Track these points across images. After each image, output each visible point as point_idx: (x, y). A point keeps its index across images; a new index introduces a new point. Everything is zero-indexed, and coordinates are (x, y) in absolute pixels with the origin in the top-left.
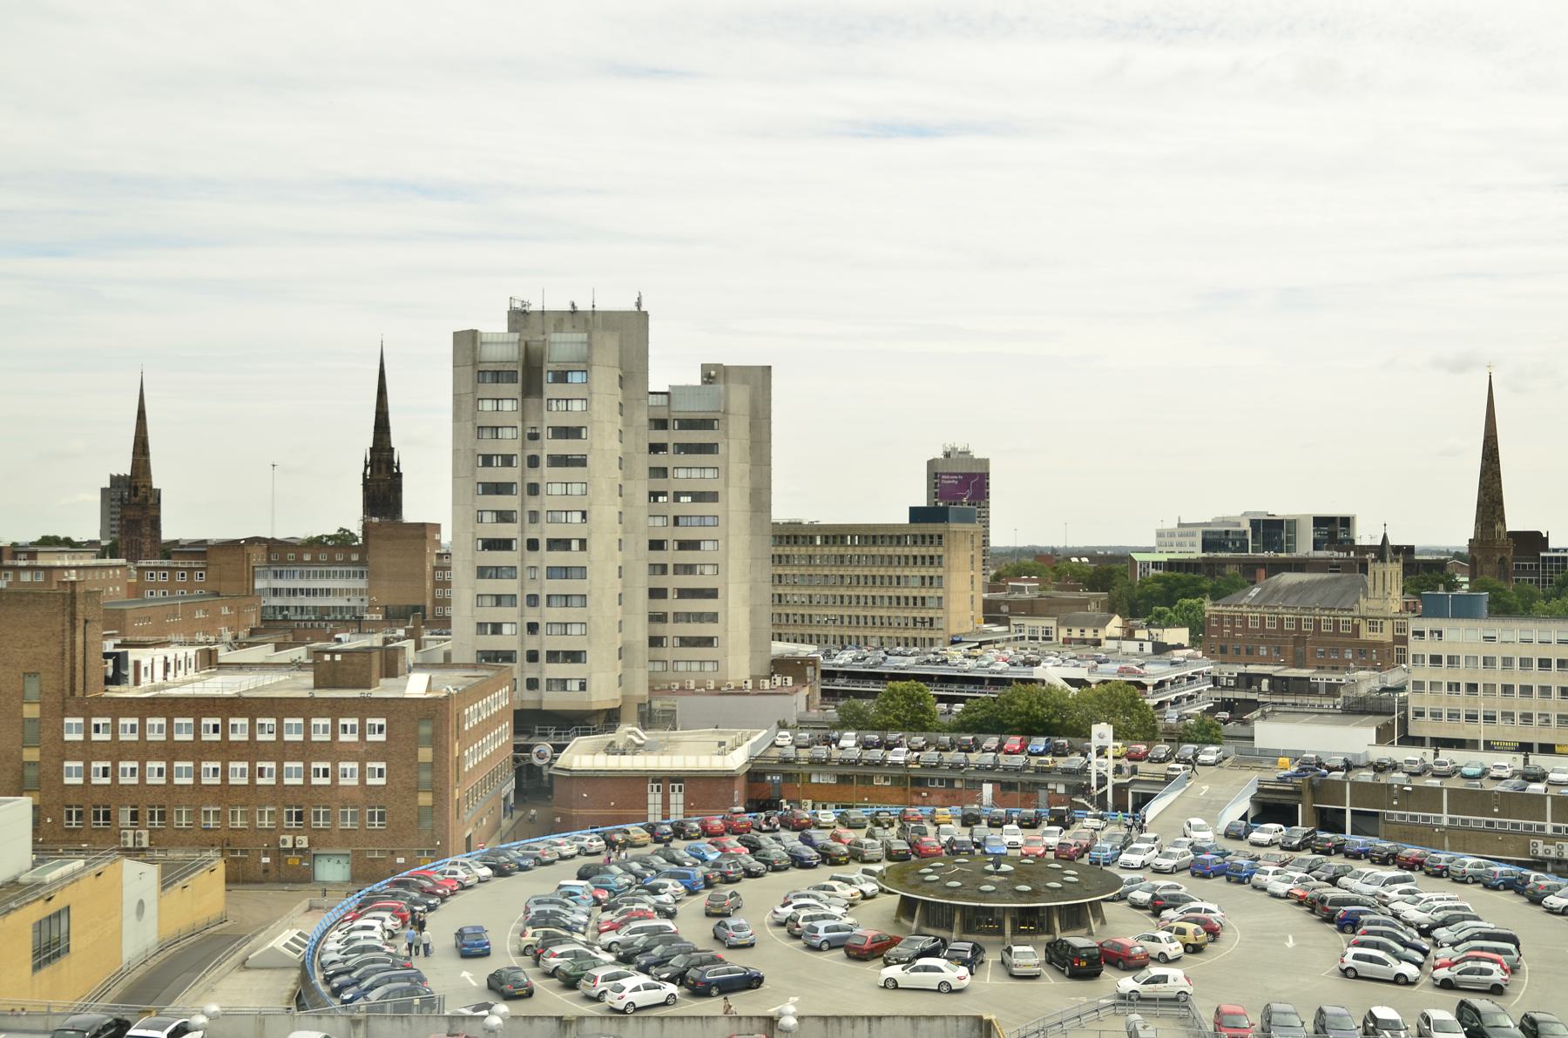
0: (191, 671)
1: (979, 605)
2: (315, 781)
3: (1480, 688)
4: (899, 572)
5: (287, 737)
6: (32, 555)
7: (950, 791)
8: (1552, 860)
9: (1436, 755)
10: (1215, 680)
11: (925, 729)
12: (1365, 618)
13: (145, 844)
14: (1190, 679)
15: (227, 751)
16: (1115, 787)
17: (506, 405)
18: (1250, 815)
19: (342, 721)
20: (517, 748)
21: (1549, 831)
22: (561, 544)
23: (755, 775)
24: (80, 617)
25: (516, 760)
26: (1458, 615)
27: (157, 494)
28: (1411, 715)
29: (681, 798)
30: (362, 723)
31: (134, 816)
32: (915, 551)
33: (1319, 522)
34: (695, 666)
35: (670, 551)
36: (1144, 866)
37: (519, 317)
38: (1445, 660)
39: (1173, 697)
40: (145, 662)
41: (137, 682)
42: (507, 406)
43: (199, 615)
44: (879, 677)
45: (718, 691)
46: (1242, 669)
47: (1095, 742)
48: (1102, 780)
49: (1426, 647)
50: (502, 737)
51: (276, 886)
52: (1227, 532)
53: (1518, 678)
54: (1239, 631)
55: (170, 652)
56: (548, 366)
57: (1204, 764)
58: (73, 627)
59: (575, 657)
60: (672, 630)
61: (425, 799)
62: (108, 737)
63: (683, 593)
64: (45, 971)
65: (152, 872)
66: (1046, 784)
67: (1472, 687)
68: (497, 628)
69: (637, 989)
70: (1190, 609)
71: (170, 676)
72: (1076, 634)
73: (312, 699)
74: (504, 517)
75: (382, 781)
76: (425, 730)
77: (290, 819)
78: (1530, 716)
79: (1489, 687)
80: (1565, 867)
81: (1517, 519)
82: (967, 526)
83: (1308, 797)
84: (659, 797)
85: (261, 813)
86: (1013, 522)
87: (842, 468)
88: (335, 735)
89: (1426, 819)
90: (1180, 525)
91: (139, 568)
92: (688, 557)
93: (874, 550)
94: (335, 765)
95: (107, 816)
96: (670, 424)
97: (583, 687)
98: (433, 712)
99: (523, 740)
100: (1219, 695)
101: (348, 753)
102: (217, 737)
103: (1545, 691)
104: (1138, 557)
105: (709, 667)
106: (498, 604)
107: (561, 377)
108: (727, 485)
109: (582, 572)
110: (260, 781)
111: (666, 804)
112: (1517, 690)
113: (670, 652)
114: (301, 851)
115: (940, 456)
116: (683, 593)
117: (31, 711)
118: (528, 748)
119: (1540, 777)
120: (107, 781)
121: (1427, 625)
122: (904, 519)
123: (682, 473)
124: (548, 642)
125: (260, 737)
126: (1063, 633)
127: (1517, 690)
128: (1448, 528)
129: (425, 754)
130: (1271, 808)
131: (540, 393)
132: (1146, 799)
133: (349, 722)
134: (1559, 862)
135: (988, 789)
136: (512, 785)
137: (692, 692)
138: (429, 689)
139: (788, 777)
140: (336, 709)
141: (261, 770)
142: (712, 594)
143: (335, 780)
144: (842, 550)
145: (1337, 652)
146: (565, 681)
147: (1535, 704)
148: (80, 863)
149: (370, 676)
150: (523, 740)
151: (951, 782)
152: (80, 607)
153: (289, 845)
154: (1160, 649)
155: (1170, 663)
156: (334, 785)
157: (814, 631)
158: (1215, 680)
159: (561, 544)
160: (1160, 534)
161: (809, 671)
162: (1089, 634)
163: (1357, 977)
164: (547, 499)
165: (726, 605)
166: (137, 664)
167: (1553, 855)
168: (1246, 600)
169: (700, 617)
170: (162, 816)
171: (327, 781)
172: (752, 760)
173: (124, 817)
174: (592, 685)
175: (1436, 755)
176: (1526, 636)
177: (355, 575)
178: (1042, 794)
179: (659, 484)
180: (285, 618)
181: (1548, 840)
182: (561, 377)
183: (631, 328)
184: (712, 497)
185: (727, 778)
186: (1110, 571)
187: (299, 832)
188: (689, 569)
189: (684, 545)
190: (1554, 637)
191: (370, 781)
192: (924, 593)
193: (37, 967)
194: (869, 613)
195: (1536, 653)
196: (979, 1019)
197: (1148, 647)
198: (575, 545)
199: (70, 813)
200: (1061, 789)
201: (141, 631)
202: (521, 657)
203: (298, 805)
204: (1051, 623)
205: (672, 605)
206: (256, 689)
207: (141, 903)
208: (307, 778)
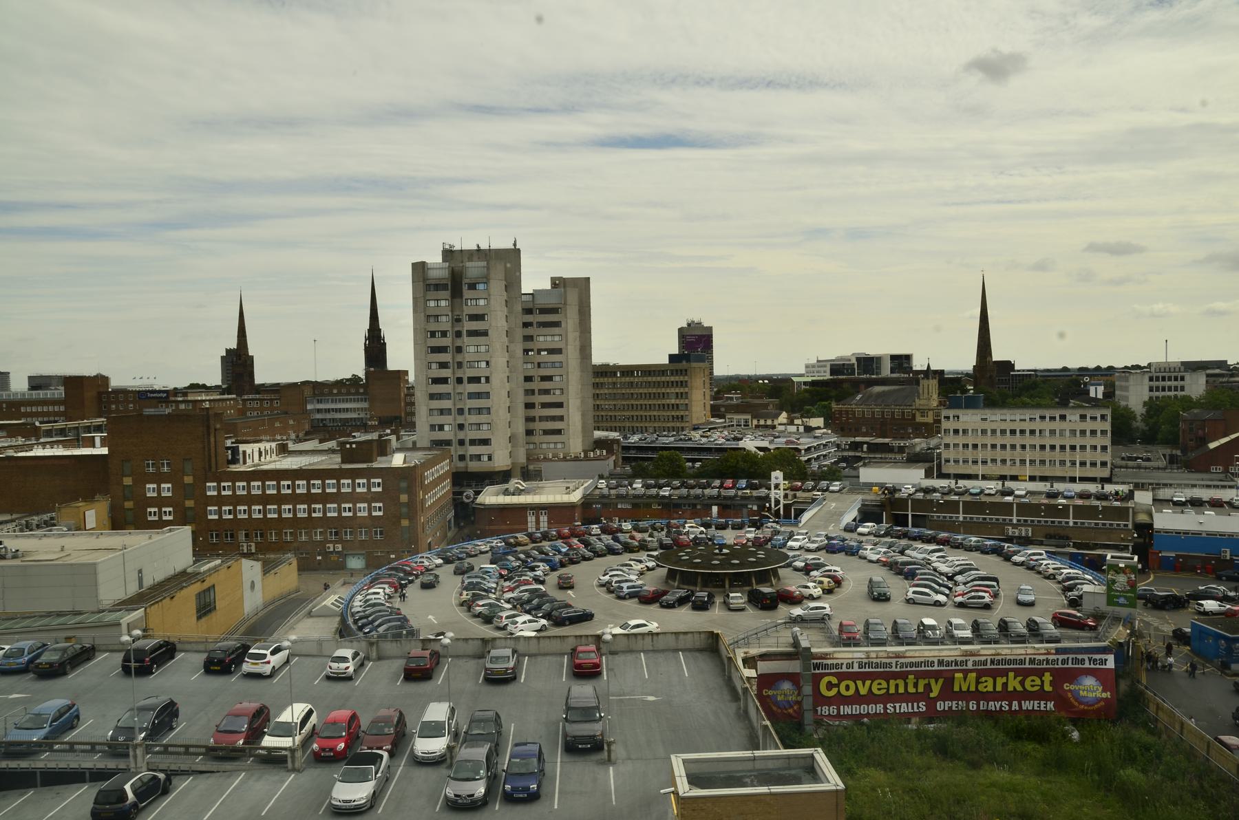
0: (274, 456)
1: (708, 408)
2: (344, 514)
6: (185, 394)
10: (838, 446)
15: (295, 499)
20: (454, 493)
22: (476, 380)
23: (587, 502)
25: (454, 500)
29: (546, 518)
31: (247, 536)
32: (673, 379)
33: (893, 358)
34: (552, 446)
36: (800, 548)
37: (448, 254)
40: (249, 451)
41: (245, 462)
45: (565, 459)
47: (773, 482)
48: (777, 502)
50: (446, 486)
53: (999, 441)
55: (262, 446)
56: (465, 281)
57: (833, 492)
58: (209, 434)
59: (486, 442)
62: (230, 493)
63: (545, 405)
64: (204, 619)
65: (258, 566)
67: (975, 446)
68: (441, 428)
70: (825, 407)
72: (762, 422)
74: (443, 365)
75: (381, 514)
76: (404, 485)
81: (998, 355)
82: (701, 364)
86: (728, 361)
87: (629, 336)
88: (354, 489)
92: (546, 385)
93: (650, 379)
94: (355, 505)
97: (490, 458)
99: (457, 489)
102: (290, 491)
103: (1013, 447)
105: (559, 446)
107: (472, 286)
109: (487, 395)
111: (538, 522)
113: (537, 438)
116: (545, 405)
117: (188, 480)
118: (461, 493)
119: (1011, 493)
120: (231, 517)
121: (951, 413)
122: (666, 361)
123: (541, 339)
125: (313, 491)
126: (755, 422)
128: (962, 360)
130: (866, 514)
131: (461, 297)
132: (803, 511)
133: (361, 481)
134: (1020, 537)
135: (715, 509)
136: (451, 515)
142: (560, 405)
143: (355, 513)
146: (479, 456)
147: (1008, 454)
148: (218, 562)
150: (457, 489)
151: (694, 505)
152: (212, 422)
154: (809, 429)
155: (813, 436)
157: (618, 425)
158: (838, 446)
159: (476, 380)
160: (807, 366)
161: (615, 447)
162: (769, 422)
163: (914, 603)
166: (244, 452)
169: (554, 418)
172: (584, 497)
173: (242, 537)
178: (745, 511)
180: (325, 425)
181: (1015, 526)
182: (472, 286)
183: (512, 257)
184: (558, 351)
185: (570, 507)
187: (337, 542)
188: (547, 392)
190: (1018, 417)
191: (374, 514)
193: (199, 618)
195: (1008, 426)
196: (712, 633)
197: (802, 429)
198: (483, 380)
200: (755, 508)
201: (244, 435)
202: (455, 443)
204: (749, 417)
205: (539, 412)
208: (340, 513)
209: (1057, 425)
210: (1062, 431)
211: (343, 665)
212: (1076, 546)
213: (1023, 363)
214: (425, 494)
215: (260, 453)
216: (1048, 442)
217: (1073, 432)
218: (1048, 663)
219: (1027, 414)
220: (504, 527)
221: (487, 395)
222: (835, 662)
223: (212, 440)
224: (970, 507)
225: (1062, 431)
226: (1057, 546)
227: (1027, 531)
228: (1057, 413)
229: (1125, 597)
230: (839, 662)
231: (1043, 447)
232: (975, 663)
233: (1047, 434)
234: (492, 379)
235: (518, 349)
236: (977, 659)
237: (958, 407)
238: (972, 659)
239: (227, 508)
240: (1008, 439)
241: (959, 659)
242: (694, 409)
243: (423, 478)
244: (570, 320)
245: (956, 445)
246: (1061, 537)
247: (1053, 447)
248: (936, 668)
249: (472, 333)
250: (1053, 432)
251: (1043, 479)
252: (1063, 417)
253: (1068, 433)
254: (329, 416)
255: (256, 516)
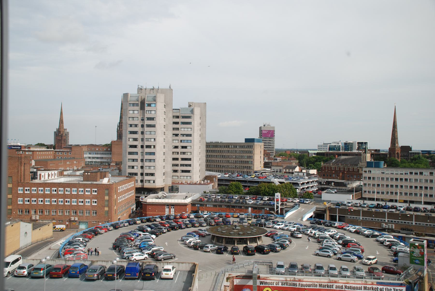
0: (56, 177)
1: (263, 163)
2: (79, 204)
3: (380, 185)
4: (242, 155)
5: (73, 193)
6: (29, 148)
7: (241, 209)
8: (387, 229)
9: (364, 202)
10: (320, 183)
11: (239, 194)
12: (361, 167)
13: (38, 219)
14: (311, 182)
15: (58, 196)
16: (281, 209)
17: (134, 113)
18: (313, 216)
19: (86, 189)
20: (136, 197)
21: (386, 221)
23: (193, 204)
24: (23, 163)
25: (136, 200)
26: (375, 167)
27: (68, 133)
28: (363, 192)
29: (173, 210)
30: (91, 190)
31: (35, 212)
32: (213, 149)
33: (358, 143)
34: (185, 177)
35: (179, 149)
36: (280, 229)
37: (140, 89)
38: (372, 178)
39: (306, 187)
41: (40, 179)
42: (136, 112)
43: (68, 163)
44: (234, 181)
45: (190, 184)
46: (327, 180)
47: (276, 197)
48: (277, 207)
49: (367, 175)
50: (132, 193)
51: (70, 230)
52: (335, 146)
53: (390, 183)
54: (329, 170)
55: (53, 172)
56: (146, 102)
57: (305, 203)
58: (21, 165)
59: (152, 175)
60: (180, 168)
61: (106, 209)
62: (29, 192)
63: (183, 159)
65: (30, 226)
66: (264, 208)
67: (378, 185)
68: (133, 167)
69: (137, 256)
70: (319, 165)
71: (50, 178)
72: (287, 171)
73: (79, 183)
74: (135, 140)
75: (96, 204)
76: (106, 192)
77: (87, 213)
78: (393, 192)
79: (383, 185)
80: (390, 230)
83: (328, 212)
84: (168, 209)
85: (66, 212)
86: (281, 143)
88: (84, 193)
89: (356, 218)
90: (324, 144)
91: (56, 152)
92: (184, 150)
93: (242, 149)
94: (84, 200)
95: (29, 212)
96: (180, 117)
97: (154, 182)
98: (108, 188)
99: (138, 195)
100: (320, 186)
101: (88, 197)
102: (56, 193)
103: (397, 186)
104: (310, 152)
105: (189, 178)
106: (133, 161)
108: (194, 132)
109: (154, 154)
110: (66, 204)
111: (170, 211)
112: (390, 186)
114: (76, 221)
115: (262, 126)
116: (183, 159)
118: (139, 197)
119: (396, 208)
120: (42, 203)
121: (367, 169)
123: (183, 129)
124: (146, 171)
125: (66, 193)
126: (284, 170)
127: (390, 186)
128: (384, 146)
129: (107, 198)
130: (319, 215)
132: (287, 212)
133: (61, 189)
134: (389, 229)
135: (250, 209)
136: (134, 207)
137: (184, 184)
138: (109, 181)
139: (201, 205)
140: (85, 186)
141: (66, 201)
142: (190, 159)
143: (85, 204)
144: (228, 149)
145: (352, 176)
147: (394, 190)
148: (9, 223)
149: (97, 179)
150: (138, 195)
151: (241, 207)
152: (23, 160)
153: (73, 220)
154: (308, 174)
155: (308, 178)
156: (84, 205)
157: (210, 169)
158: (320, 183)
160: (319, 146)
161: (214, 179)
162: (291, 171)
163: (319, 256)
164: (145, 135)
165: (193, 162)
166: (40, 175)
167: (387, 227)
168: (331, 163)
169: (186, 165)
170: (42, 212)
171: (82, 204)
172: (193, 201)
173: (32, 212)
174: (156, 182)
175: (364, 202)
176: (397, 173)
177: (109, 154)
178: (263, 210)
179: (176, 132)
180: (91, 164)
181: (386, 223)
182: (149, 105)
184: (190, 135)
185: (185, 205)
186: (304, 155)
187: (75, 216)
188: (184, 153)
189: (183, 147)
190: (399, 173)
191: (93, 204)
192: (248, 160)
194: (219, 164)
195: (394, 177)
196: (194, 264)
197: (305, 174)
198: (152, 147)
199: (19, 211)
200: (268, 209)
202: (139, 174)
203: (76, 210)
204: (282, 168)
205: (180, 162)
206: (69, 181)
207: (26, 233)
208: (78, 203)
209: (418, 177)
210: (421, 180)
211: (22, 271)
212: (416, 234)
213: (416, 148)
214: (118, 196)
215: (49, 175)
216: (414, 185)
217: (426, 181)
218: (328, 287)
219: (404, 171)
220: (154, 213)
221: (154, 154)
222: (270, 281)
223: (23, 168)
224: (365, 213)
225: (421, 180)
226: (406, 234)
227: (392, 226)
228: (418, 171)
229: (419, 260)
230: (272, 281)
231: (411, 187)
232: (337, 287)
233: (413, 181)
234: (156, 147)
235: (170, 133)
236: (338, 284)
237: (372, 167)
238: (335, 284)
239: (27, 199)
240: (394, 183)
241: (329, 284)
242: (255, 164)
243: (117, 190)
244: (196, 120)
245: (369, 184)
246: (408, 230)
247: (416, 187)
248: (318, 288)
249: (149, 126)
250: (416, 180)
251: (382, 200)
252: (421, 173)
253: (424, 181)
254: (94, 160)
255: (40, 203)
